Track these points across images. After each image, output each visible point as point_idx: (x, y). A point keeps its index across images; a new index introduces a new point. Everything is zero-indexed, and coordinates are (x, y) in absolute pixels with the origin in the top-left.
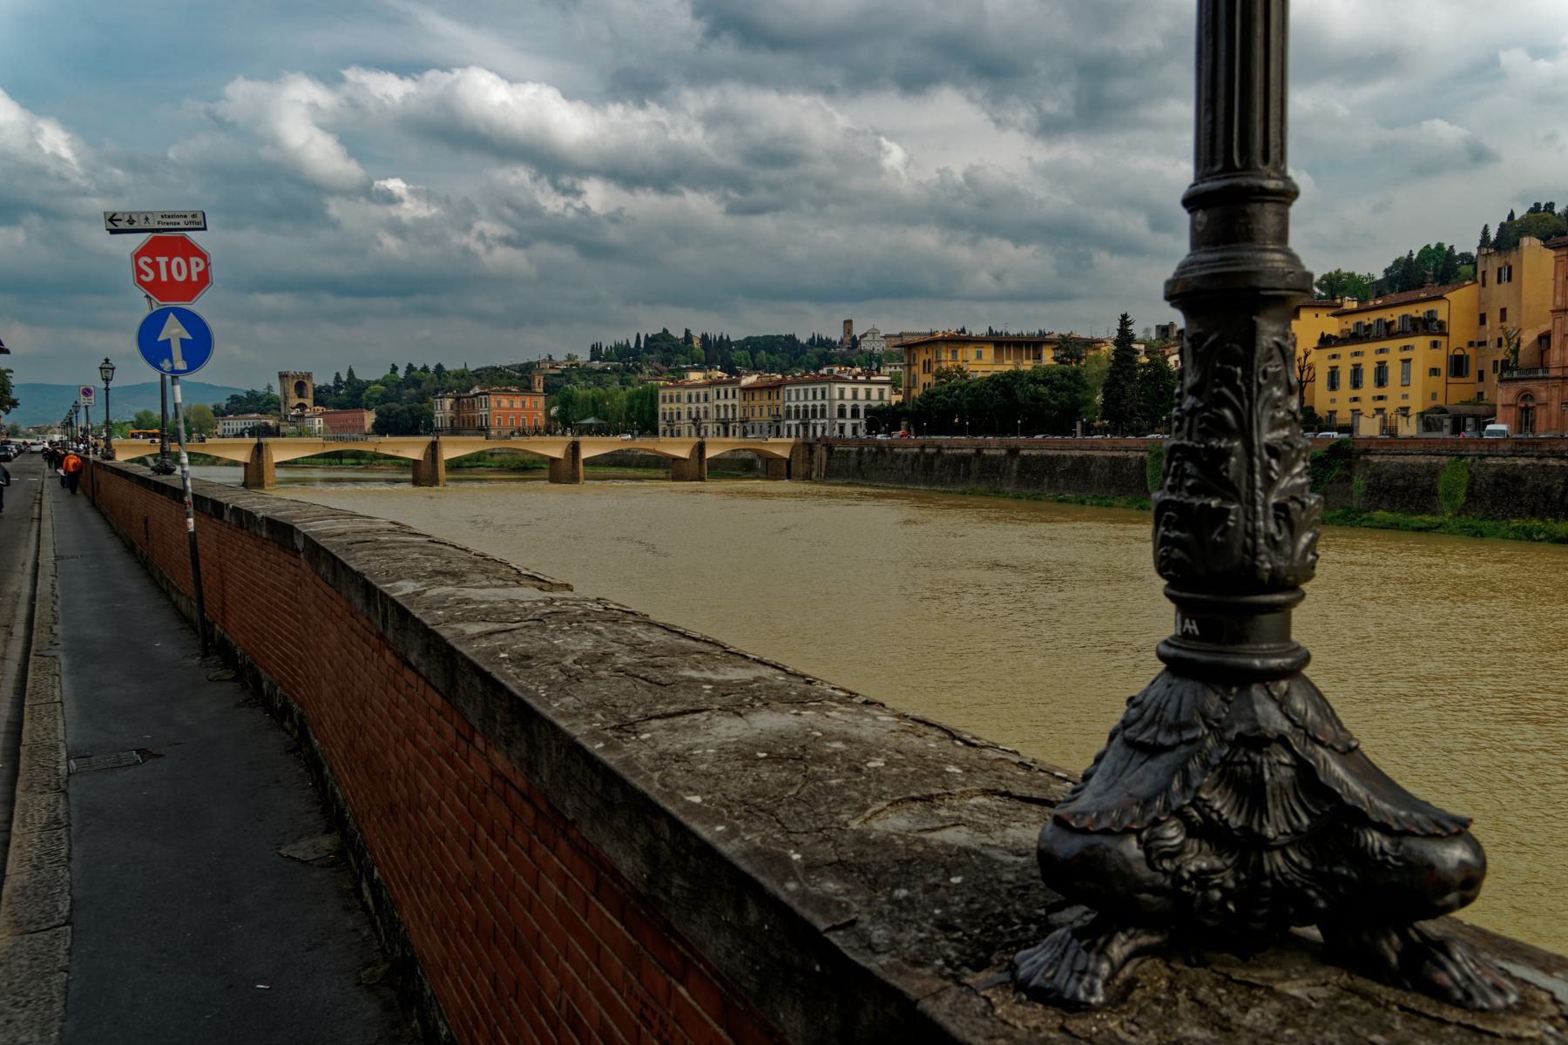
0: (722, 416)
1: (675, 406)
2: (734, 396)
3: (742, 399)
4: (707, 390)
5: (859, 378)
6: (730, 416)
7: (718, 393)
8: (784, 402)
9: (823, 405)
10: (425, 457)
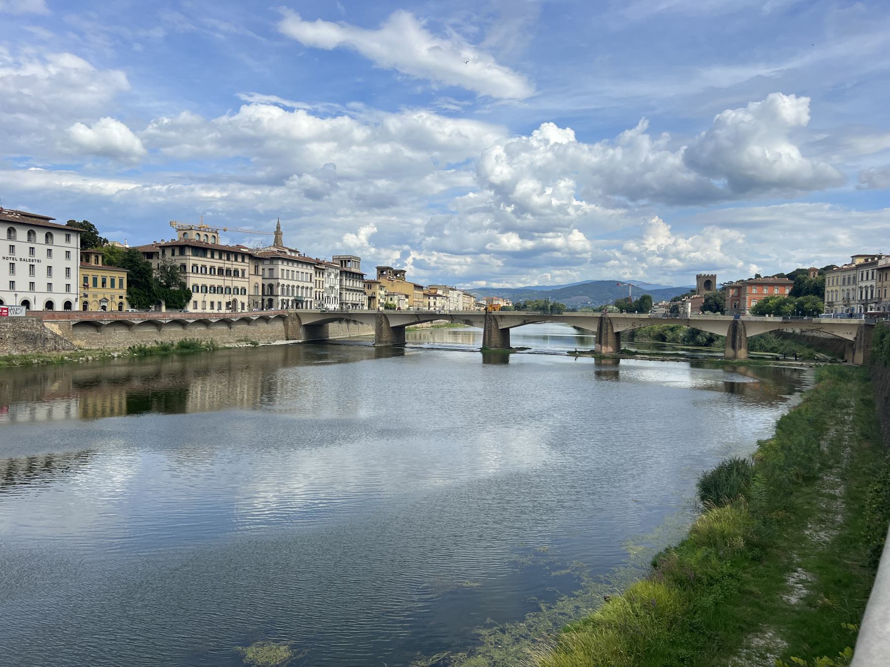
0: (864, 298)
3: (878, 280)
6: (869, 298)
7: (862, 274)
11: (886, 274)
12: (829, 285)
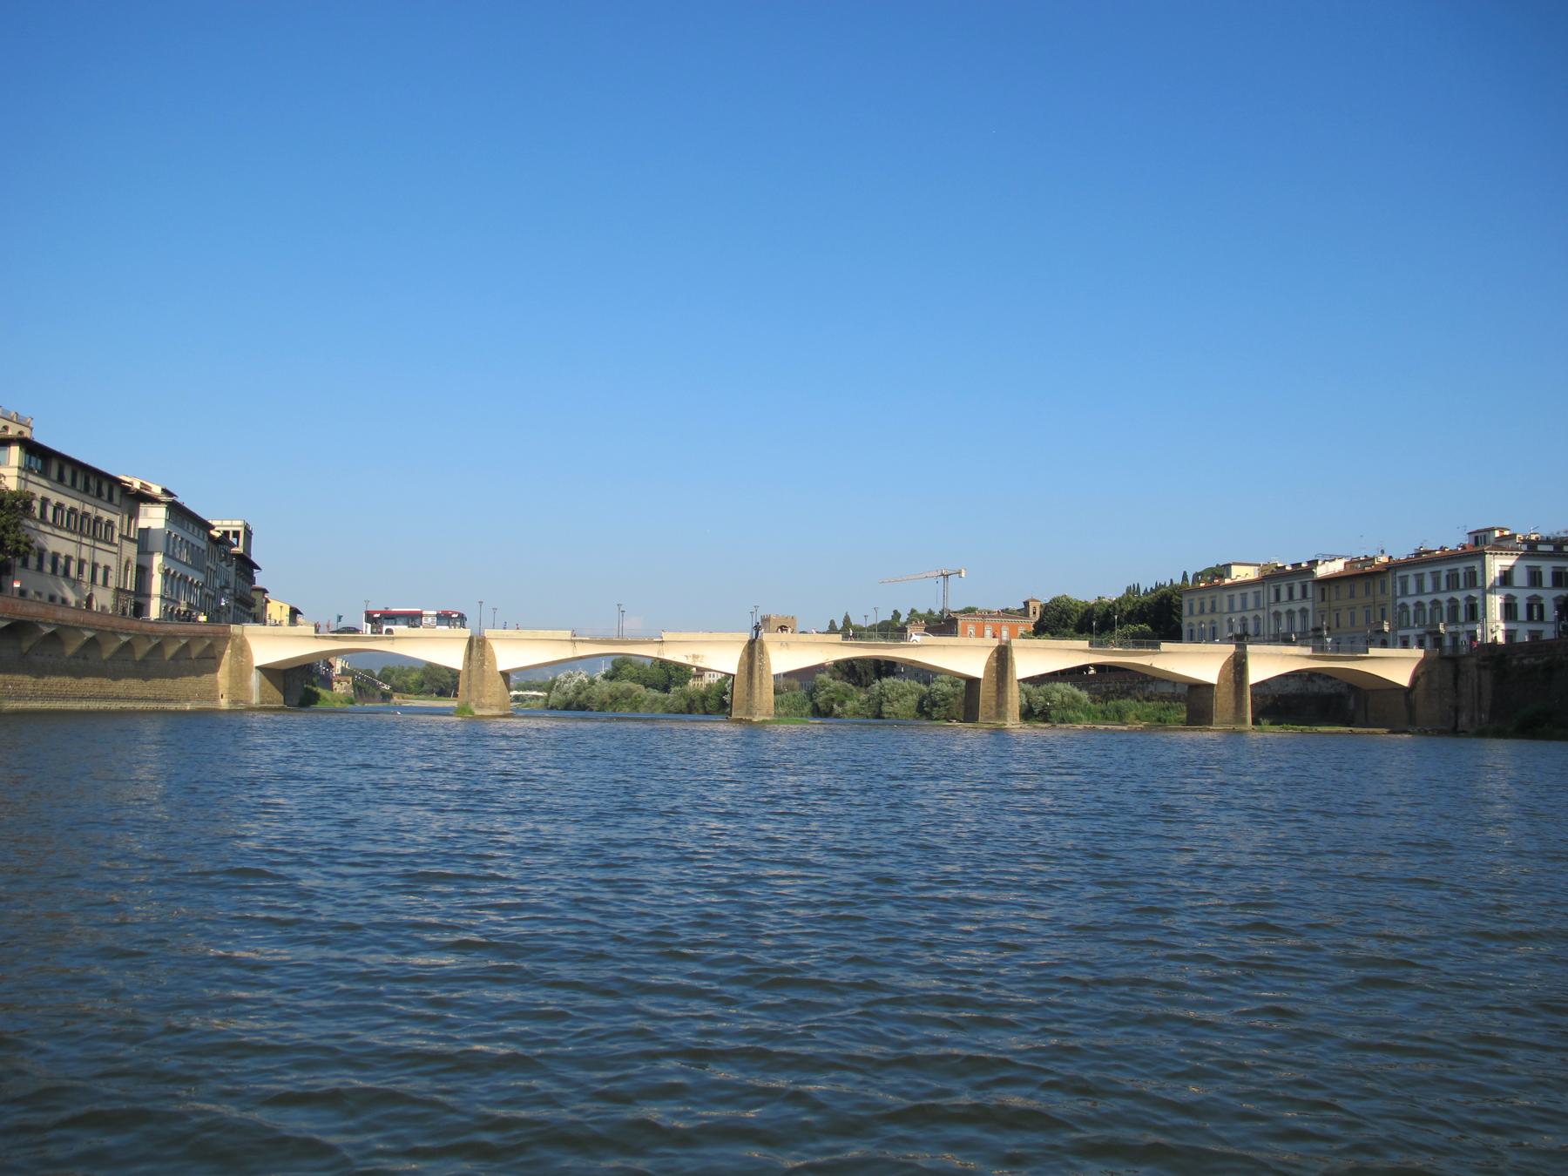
1: (1206, 618)
2: (1304, 595)
3: (1319, 597)
4: (1260, 588)
5: (1541, 548)
8: (1396, 597)
9: (1470, 598)
10: (739, 670)
11: (1337, 587)
12: (1191, 612)
